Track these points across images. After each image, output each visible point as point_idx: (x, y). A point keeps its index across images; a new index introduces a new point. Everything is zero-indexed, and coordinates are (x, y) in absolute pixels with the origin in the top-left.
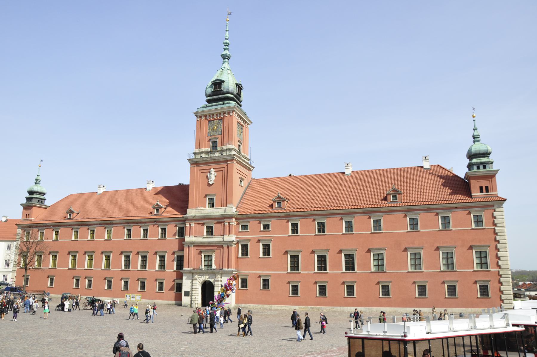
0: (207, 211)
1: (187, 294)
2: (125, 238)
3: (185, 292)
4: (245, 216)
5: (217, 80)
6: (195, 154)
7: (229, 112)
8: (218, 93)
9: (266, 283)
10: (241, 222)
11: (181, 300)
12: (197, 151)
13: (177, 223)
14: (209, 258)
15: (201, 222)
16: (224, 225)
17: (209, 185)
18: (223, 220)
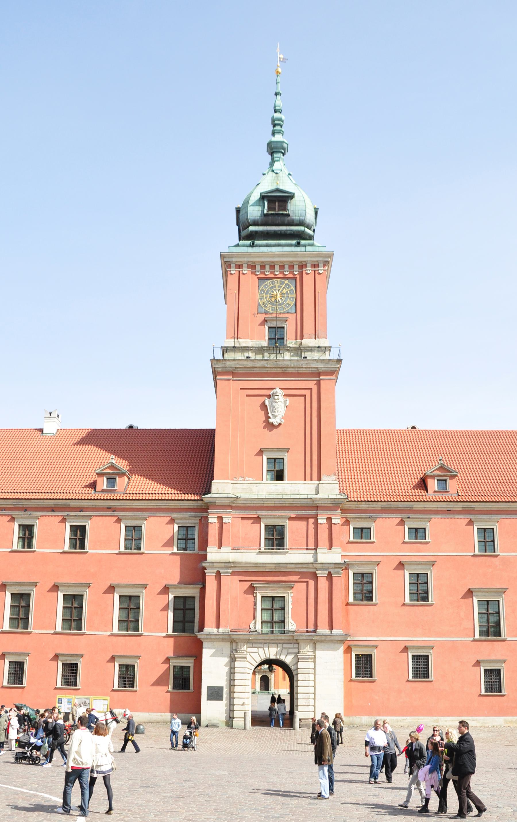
0: (267, 489)
1: (215, 694)
2: (15, 548)
3: (209, 688)
4: (363, 506)
5: (278, 190)
6: (225, 350)
7: (315, 266)
8: (278, 219)
9: (421, 666)
10: (355, 519)
11: (197, 711)
12: (231, 343)
13: (175, 514)
14: (276, 606)
15: (253, 514)
16: (316, 524)
17: (270, 426)
18: (312, 513)
